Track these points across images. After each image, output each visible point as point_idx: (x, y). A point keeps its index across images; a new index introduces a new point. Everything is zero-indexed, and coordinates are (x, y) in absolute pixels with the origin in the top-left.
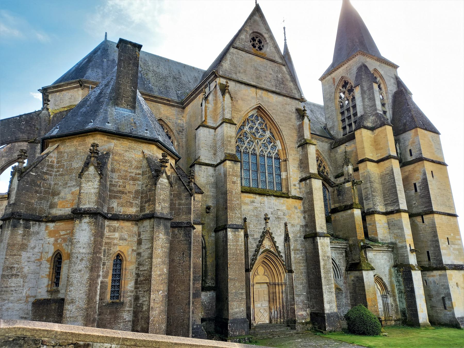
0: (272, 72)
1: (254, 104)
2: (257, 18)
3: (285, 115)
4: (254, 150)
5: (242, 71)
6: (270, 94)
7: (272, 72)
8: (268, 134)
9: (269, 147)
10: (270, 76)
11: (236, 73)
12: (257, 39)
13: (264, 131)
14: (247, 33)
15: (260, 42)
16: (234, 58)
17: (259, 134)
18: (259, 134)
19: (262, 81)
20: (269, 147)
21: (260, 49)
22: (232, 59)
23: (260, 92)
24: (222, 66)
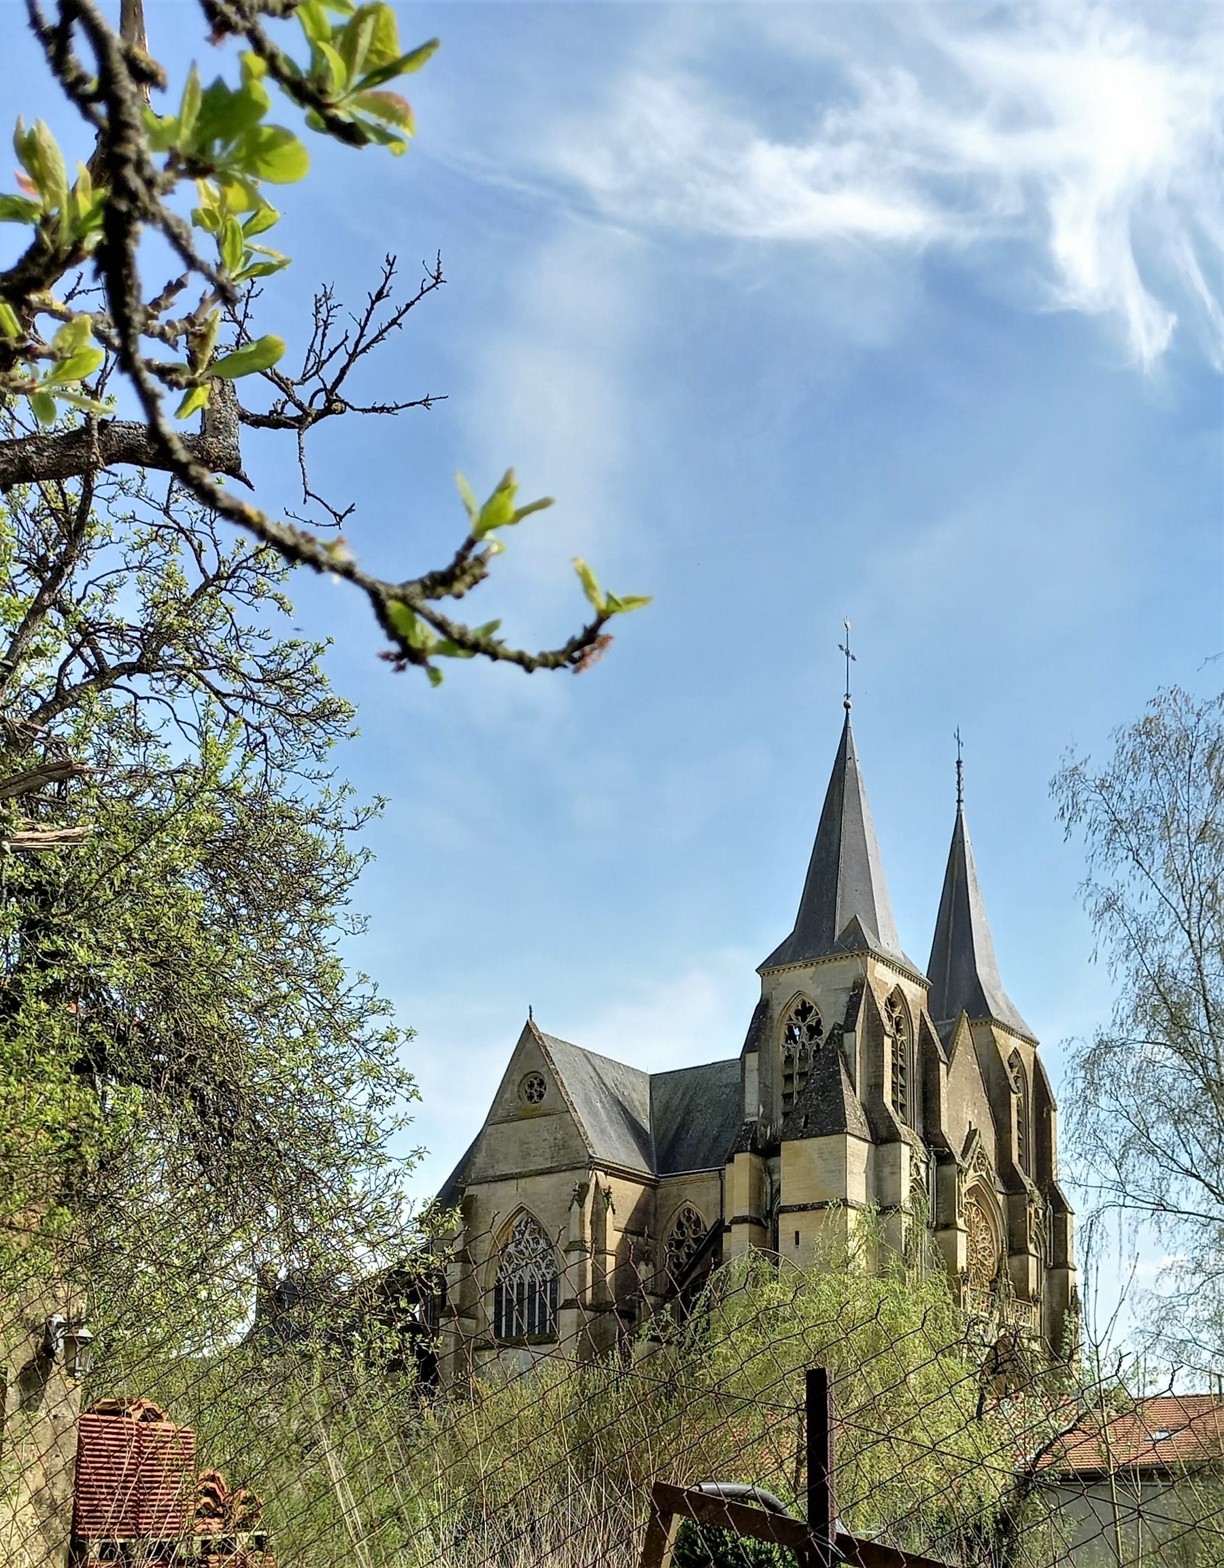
0: (547, 1136)
1: (512, 1207)
2: (530, 1046)
3: (560, 1205)
4: (521, 1277)
5: (501, 1158)
6: (538, 1178)
7: (547, 1136)
8: (543, 1244)
9: (543, 1265)
10: (544, 1144)
11: (493, 1167)
12: (535, 1082)
13: (538, 1243)
14: (514, 1084)
15: (541, 1083)
19: (530, 1161)
20: (543, 1265)
21: (541, 1096)
22: (489, 1144)
23: (522, 1182)
24: (474, 1164)
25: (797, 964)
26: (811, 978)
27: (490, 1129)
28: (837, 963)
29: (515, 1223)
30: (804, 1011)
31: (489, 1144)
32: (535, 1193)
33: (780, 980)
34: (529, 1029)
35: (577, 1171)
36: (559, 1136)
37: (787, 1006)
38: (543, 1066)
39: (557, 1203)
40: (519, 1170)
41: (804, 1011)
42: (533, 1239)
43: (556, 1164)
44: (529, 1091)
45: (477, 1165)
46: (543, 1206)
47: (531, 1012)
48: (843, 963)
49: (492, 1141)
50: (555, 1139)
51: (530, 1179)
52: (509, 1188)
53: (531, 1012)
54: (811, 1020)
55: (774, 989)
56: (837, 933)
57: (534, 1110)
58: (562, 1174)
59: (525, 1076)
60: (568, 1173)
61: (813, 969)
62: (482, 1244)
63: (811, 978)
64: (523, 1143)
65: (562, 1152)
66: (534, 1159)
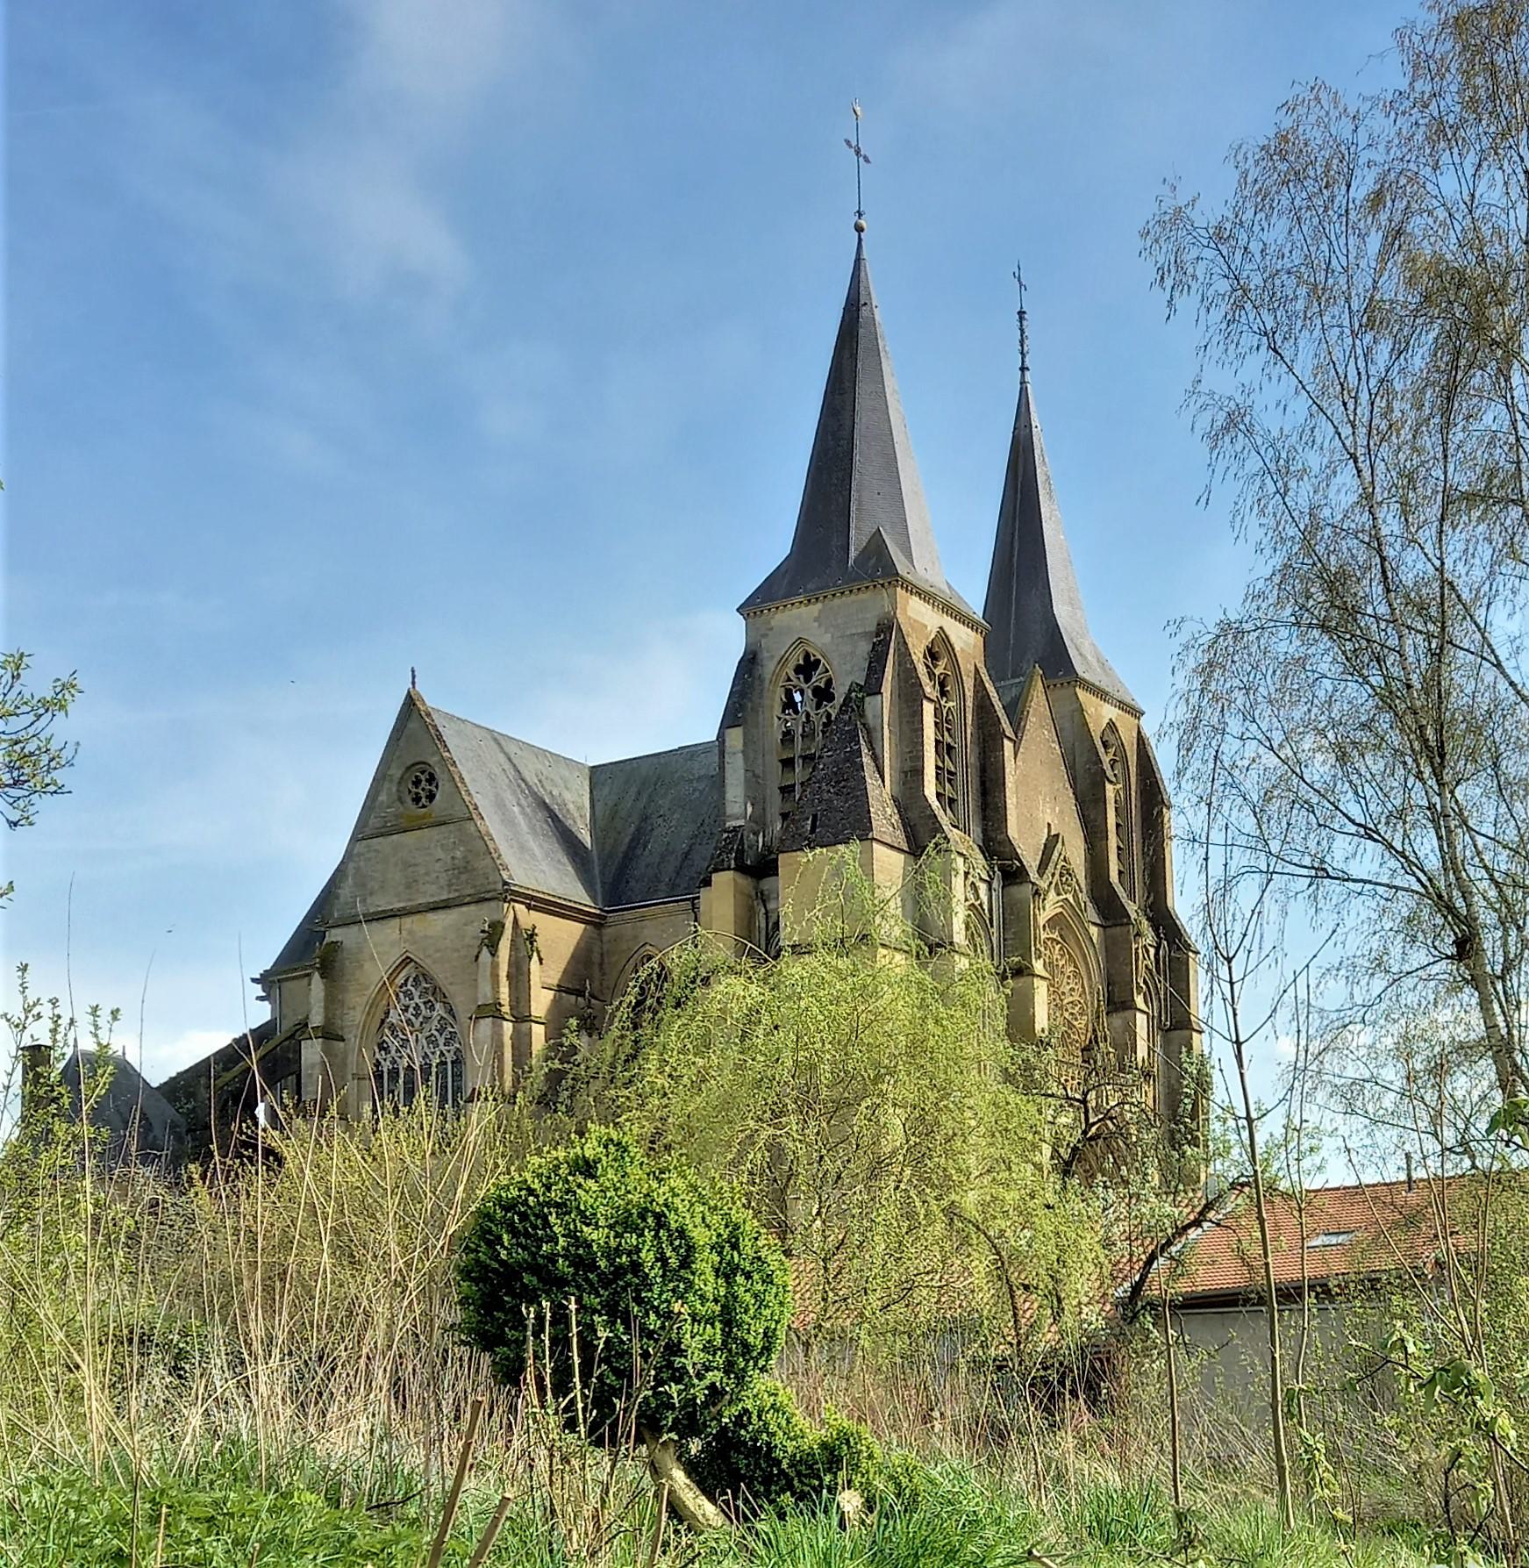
0: (440, 854)
1: (395, 957)
2: (413, 725)
3: (463, 952)
6: (430, 916)
9: (441, 1041)
13: (432, 1008)
14: (391, 781)
15: (431, 779)
16: (362, 863)
17: (421, 1019)
18: (421, 1019)
20: (441, 1041)
21: (431, 797)
22: (358, 869)
23: (408, 922)
24: (337, 897)
25: (796, 600)
26: (816, 620)
27: (360, 847)
28: (853, 597)
29: (400, 980)
30: (808, 667)
31: (358, 869)
32: (426, 937)
33: (773, 623)
34: (411, 705)
35: (486, 904)
36: (458, 854)
37: (783, 661)
38: (433, 754)
39: (458, 950)
40: (402, 905)
41: (808, 667)
42: (425, 1003)
43: (457, 894)
44: (414, 790)
45: (342, 899)
46: (438, 955)
47: (414, 677)
48: (862, 596)
49: (362, 863)
50: (453, 858)
51: (418, 917)
52: (390, 929)
53: (414, 677)
54: (818, 679)
55: (765, 636)
56: (853, 554)
57: (423, 817)
58: (464, 909)
59: (408, 768)
60: (473, 907)
61: (819, 605)
62: (351, 1012)
63: (816, 620)
64: (407, 865)
65: (463, 877)
66: (423, 888)
